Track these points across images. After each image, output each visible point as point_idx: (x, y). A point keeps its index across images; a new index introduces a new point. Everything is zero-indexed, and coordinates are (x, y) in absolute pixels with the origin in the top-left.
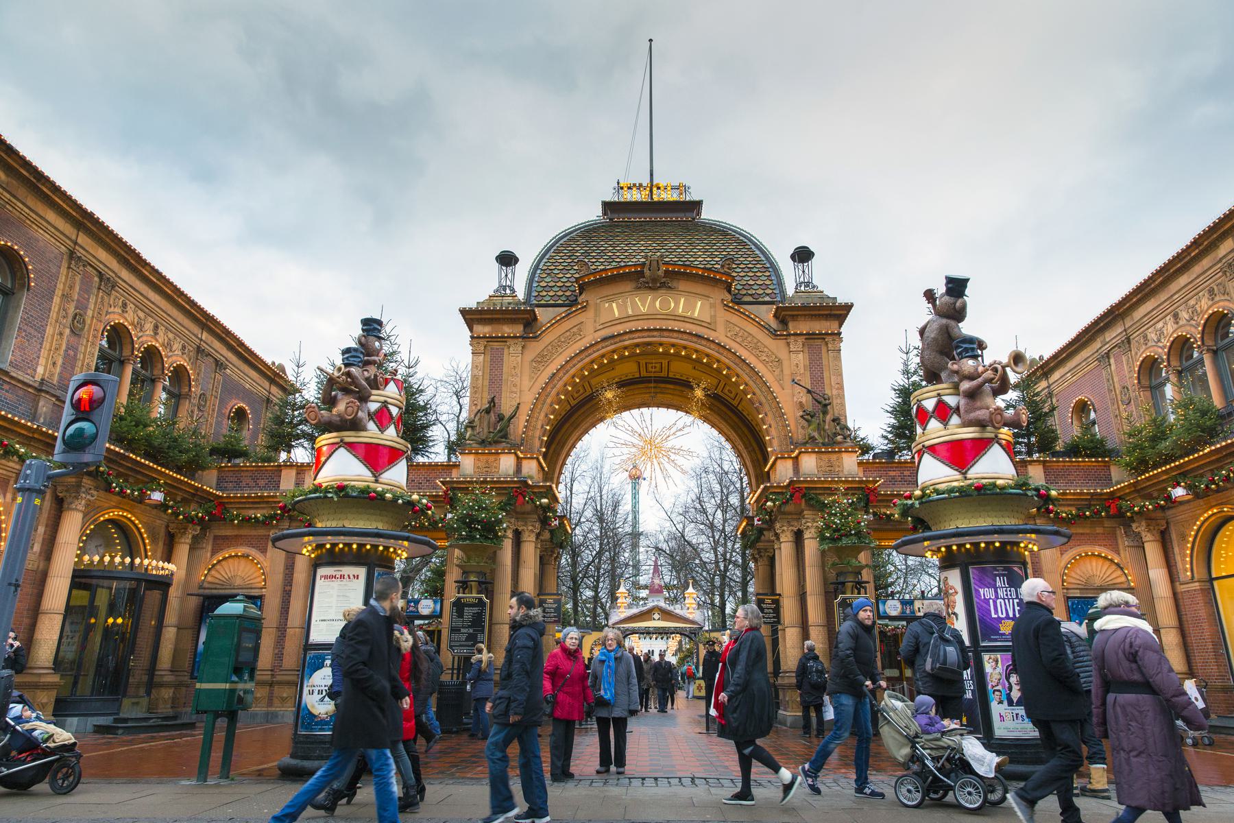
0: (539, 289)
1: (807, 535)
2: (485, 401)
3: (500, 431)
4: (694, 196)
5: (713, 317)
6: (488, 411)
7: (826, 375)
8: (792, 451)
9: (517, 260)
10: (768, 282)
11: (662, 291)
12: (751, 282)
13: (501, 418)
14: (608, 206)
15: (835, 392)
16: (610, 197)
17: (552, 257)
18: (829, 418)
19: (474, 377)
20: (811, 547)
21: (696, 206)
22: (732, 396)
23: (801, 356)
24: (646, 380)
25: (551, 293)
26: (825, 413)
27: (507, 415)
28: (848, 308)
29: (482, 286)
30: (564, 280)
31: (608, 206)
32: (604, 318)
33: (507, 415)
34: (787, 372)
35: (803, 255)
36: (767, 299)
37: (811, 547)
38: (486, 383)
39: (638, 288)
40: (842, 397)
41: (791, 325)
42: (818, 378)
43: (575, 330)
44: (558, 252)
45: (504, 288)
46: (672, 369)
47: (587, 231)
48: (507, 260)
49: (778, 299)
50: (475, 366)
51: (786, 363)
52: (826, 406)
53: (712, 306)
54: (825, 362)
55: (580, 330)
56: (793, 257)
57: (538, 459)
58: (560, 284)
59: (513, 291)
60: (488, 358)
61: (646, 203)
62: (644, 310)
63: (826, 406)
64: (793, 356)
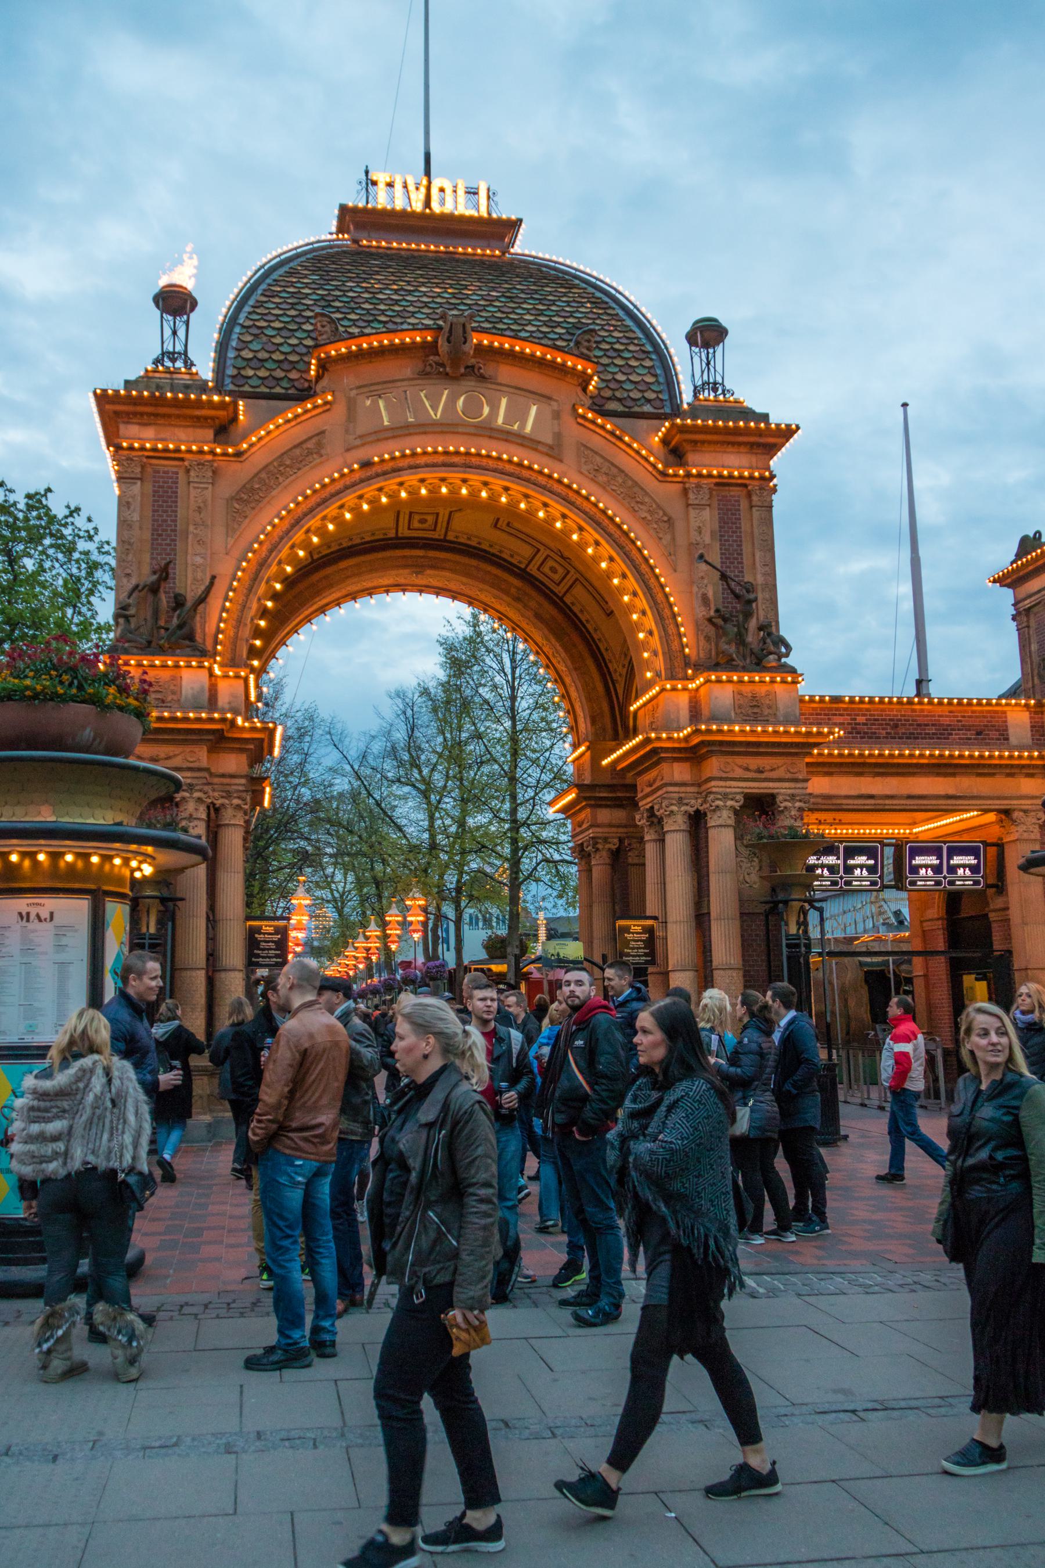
0: (241, 363)
1: (712, 821)
2: (146, 570)
3: (180, 627)
4: (505, 212)
5: (558, 436)
6: (154, 589)
7: (746, 549)
8: (692, 679)
9: (194, 304)
10: (649, 379)
11: (469, 383)
12: (620, 377)
13: (179, 602)
14: (350, 218)
15: (760, 579)
16: (356, 200)
17: (259, 304)
18: (753, 624)
19: (123, 524)
20: (722, 841)
21: (513, 226)
23: (706, 514)
24: (411, 543)
25: (262, 373)
26: (748, 615)
27: (191, 597)
28: (788, 433)
29: (132, 351)
30: (285, 349)
31: (348, 216)
32: (363, 426)
33: (191, 597)
34: (681, 541)
35: (708, 334)
36: (647, 408)
37: (722, 841)
38: (147, 535)
39: (424, 374)
40: (772, 587)
41: (691, 457)
42: (732, 553)
43: (310, 445)
44: (269, 294)
45: (173, 356)
47: (318, 259)
48: (175, 303)
49: (668, 410)
50: (124, 503)
51: (680, 526)
52: (750, 602)
53: (557, 415)
54: (745, 526)
55: (320, 445)
56: (691, 339)
57: (246, 680)
58: (277, 356)
59: (189, 364)
60: (149, 488)
61: (422, 216)
62: (437, 415)
63: (750, 602)
64: (693, 513)
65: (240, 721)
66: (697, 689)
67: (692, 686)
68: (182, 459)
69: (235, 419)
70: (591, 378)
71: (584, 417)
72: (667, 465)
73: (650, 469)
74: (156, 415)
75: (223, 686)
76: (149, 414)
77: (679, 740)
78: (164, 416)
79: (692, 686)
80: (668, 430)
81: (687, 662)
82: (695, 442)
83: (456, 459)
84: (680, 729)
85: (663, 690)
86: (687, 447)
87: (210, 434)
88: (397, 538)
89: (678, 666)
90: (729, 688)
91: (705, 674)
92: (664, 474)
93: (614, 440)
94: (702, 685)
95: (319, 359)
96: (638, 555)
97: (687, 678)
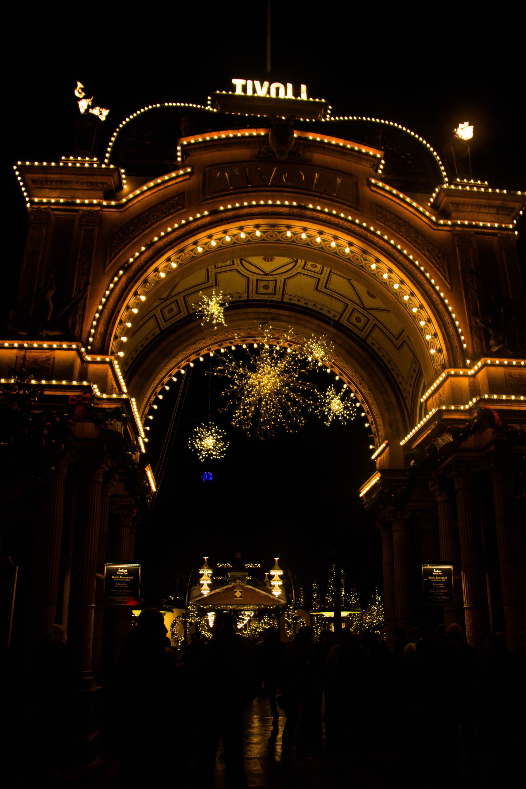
8: (470, 367)
22: (360, 325)
46: (288, 291)
57: (111, 363)
65: (97, 391)
66: (474, 376)
67: (471, 372)
68: (77, 211)
69: (122, 188)
70: (380, 160)
71: (376, 185)
72: (438, 219)
73: (427, 221)
74: (61, 182)
75: (92, 368)
76: (57, 181)
77: (464, 411)
78: (66, 182)
79: (471, 372)
80: (438, 195)
81: (464, 354)
82: (458, 204)
83: (283, 210)
84: (465, 403)
85: (449, 375)
86: (451, 208)
87: (101, 194)
88: (248, 300)
89: (456, 358)
90: (501, 370)
91: (483, 360)
92: (436, 224)
93: (398, 201)
94: (480, 369)
95: (183, 146)
96: (422, 278)
97: (465, 367)
